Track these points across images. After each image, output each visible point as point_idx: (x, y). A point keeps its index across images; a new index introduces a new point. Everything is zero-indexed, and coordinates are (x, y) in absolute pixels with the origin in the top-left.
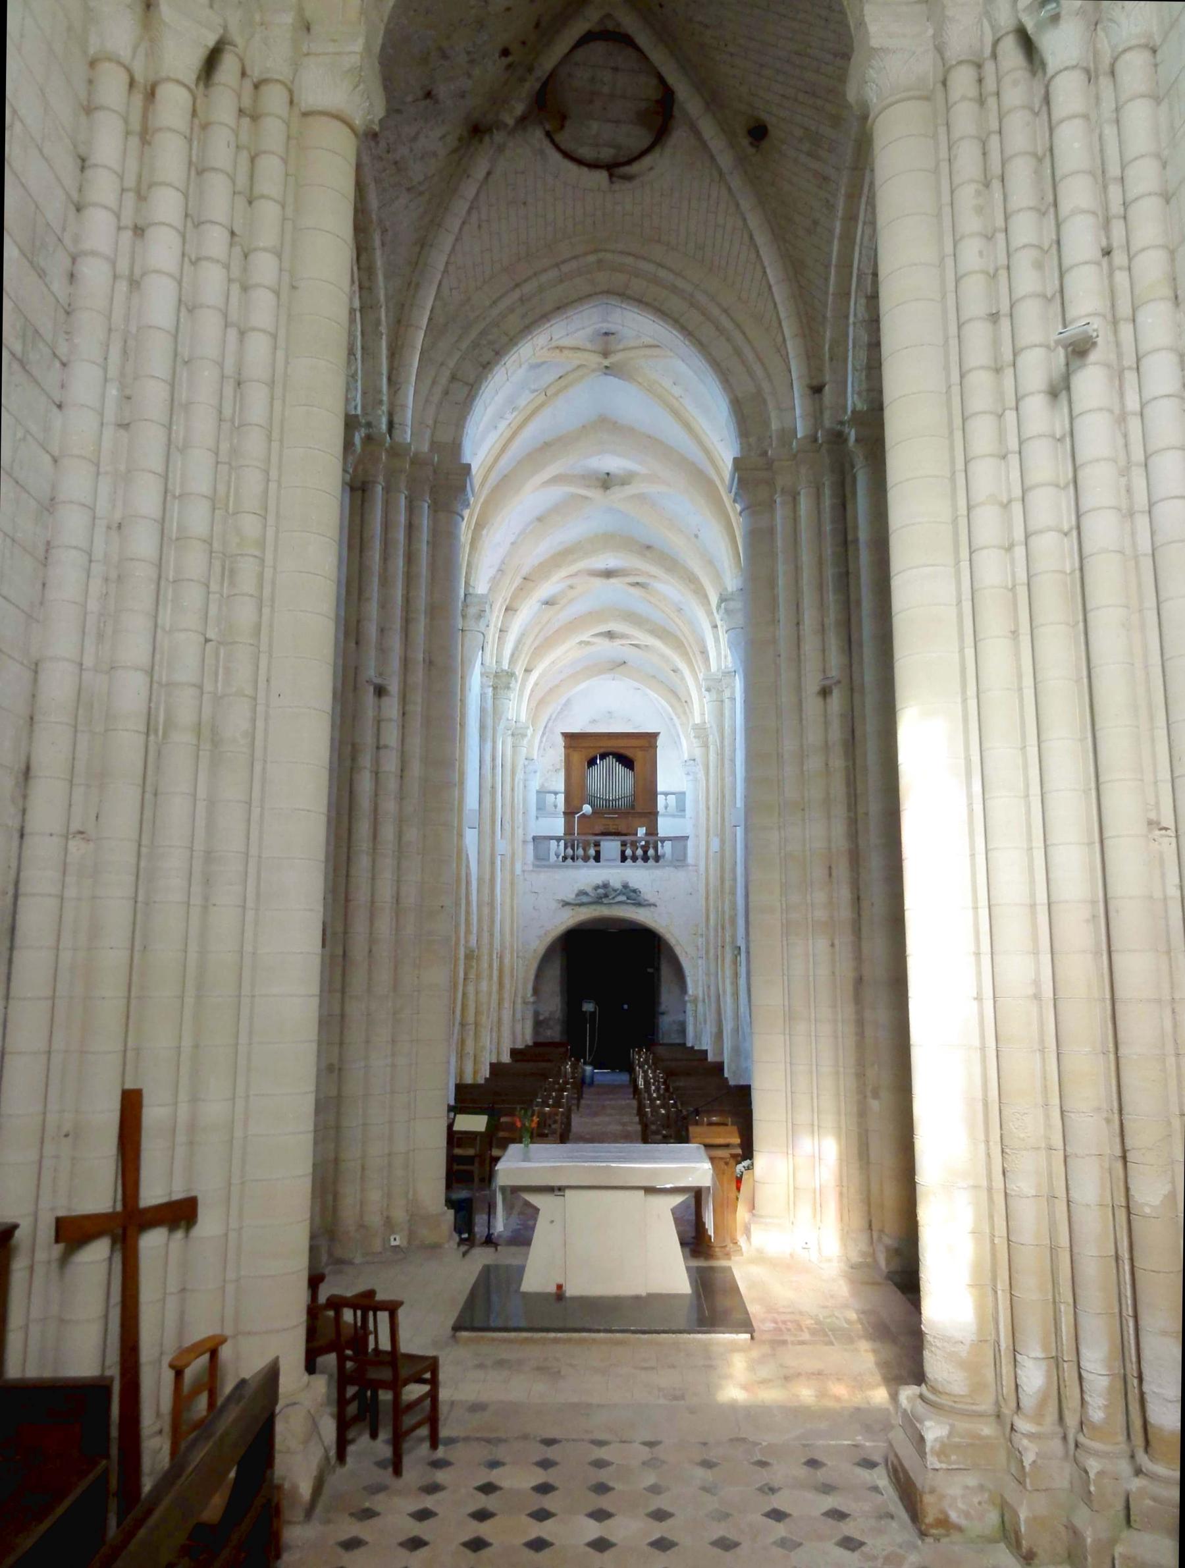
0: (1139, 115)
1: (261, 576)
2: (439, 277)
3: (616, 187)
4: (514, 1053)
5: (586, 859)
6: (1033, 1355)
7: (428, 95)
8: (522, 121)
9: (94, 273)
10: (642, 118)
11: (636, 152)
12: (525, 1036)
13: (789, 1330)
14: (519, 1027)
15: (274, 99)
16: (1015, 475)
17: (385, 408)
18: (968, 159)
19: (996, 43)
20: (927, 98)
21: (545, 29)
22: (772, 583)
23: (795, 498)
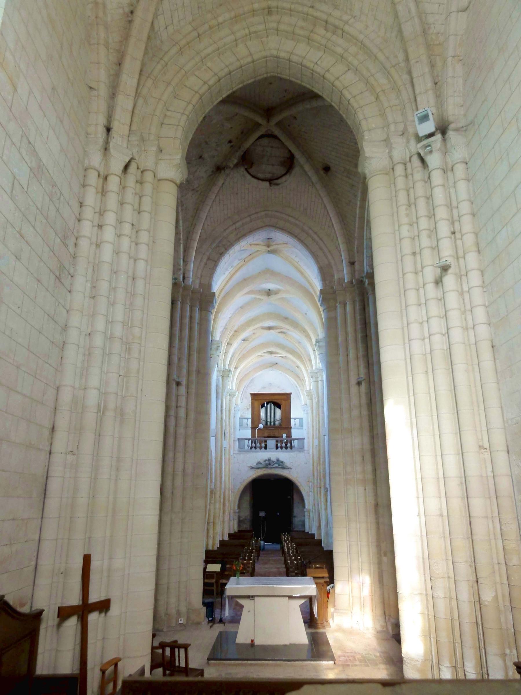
0: (462, 186)
1: (140, 351)
2: (203, 221)
3: (272, 188)
4: (230, 535)
5: (261, 448)
6: (446, 666)
7: (201, 157)
8: (236, 166)
9: (84, 244)
10: (282, 164)
11: (279, 175)
12: (235, 528)
13: (350, 660)
14: (231, 523)
15: (149, 177)
16: (424, 312)
17: (182, 271)
18: (402, 196)
19: (411, 157)
20: (387, 174)
21: (245, 134)
22: (336, 339)
23: (345, 305)
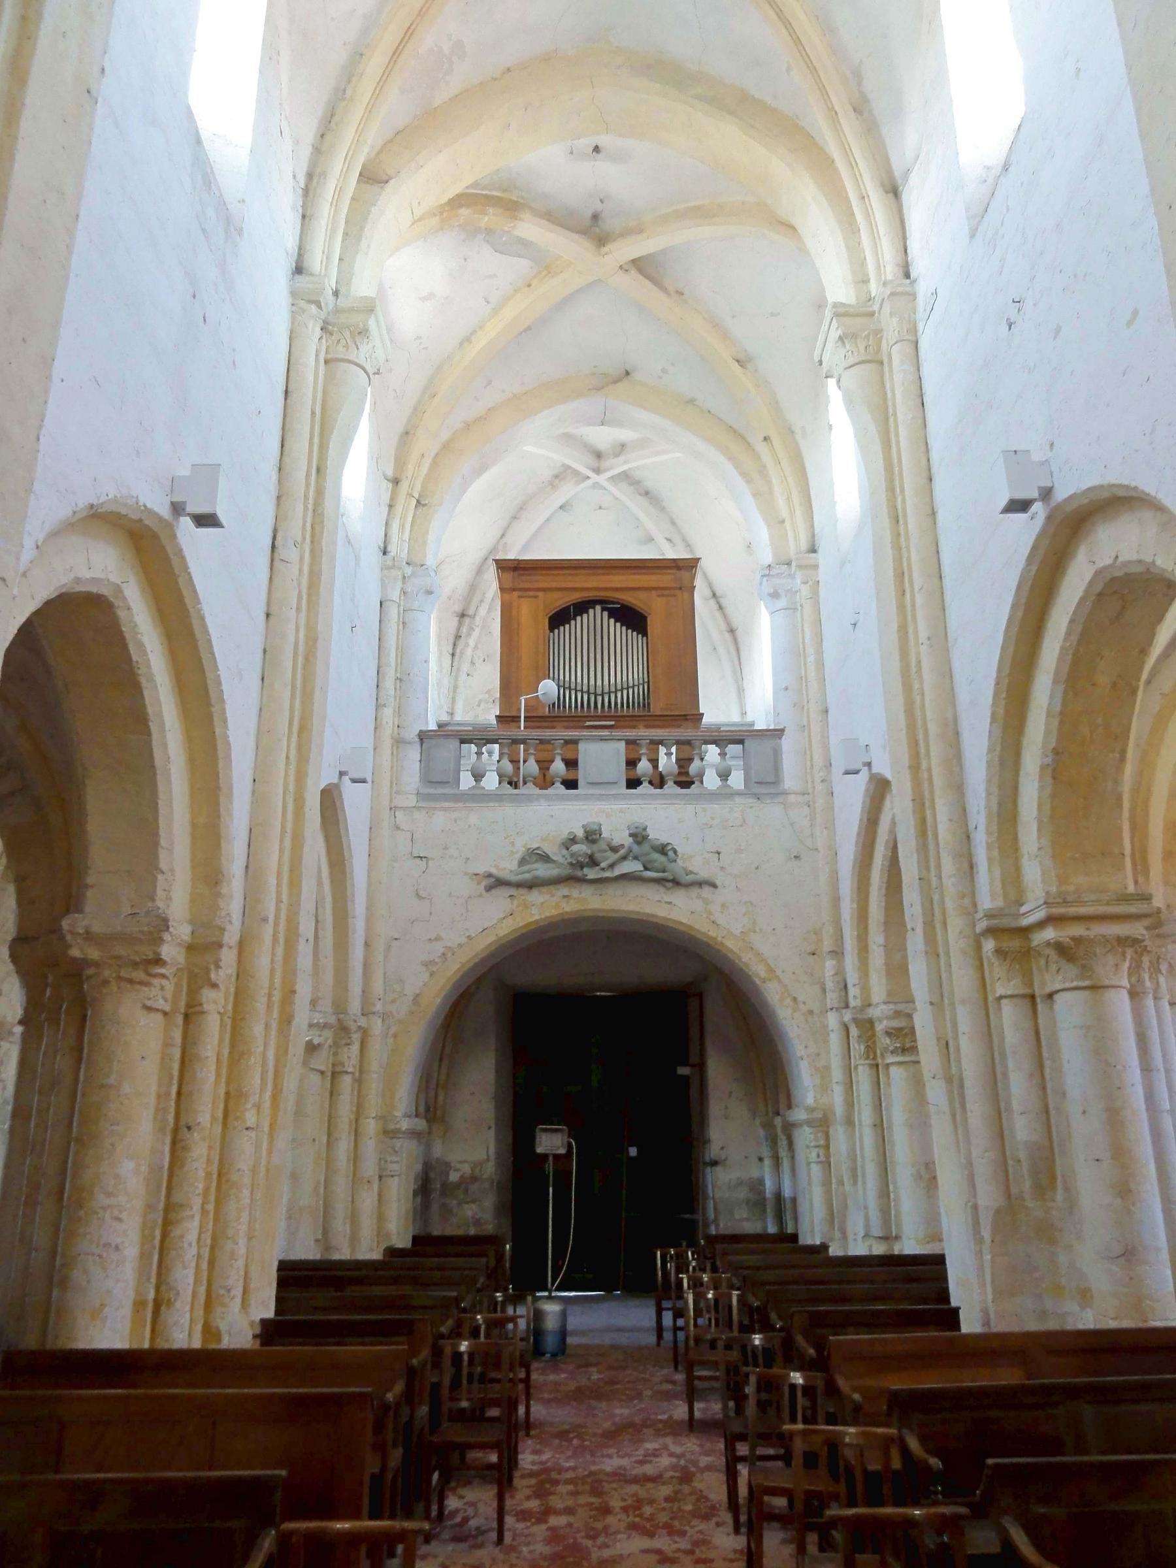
5: (544, 782)
14: (367, 1201)
